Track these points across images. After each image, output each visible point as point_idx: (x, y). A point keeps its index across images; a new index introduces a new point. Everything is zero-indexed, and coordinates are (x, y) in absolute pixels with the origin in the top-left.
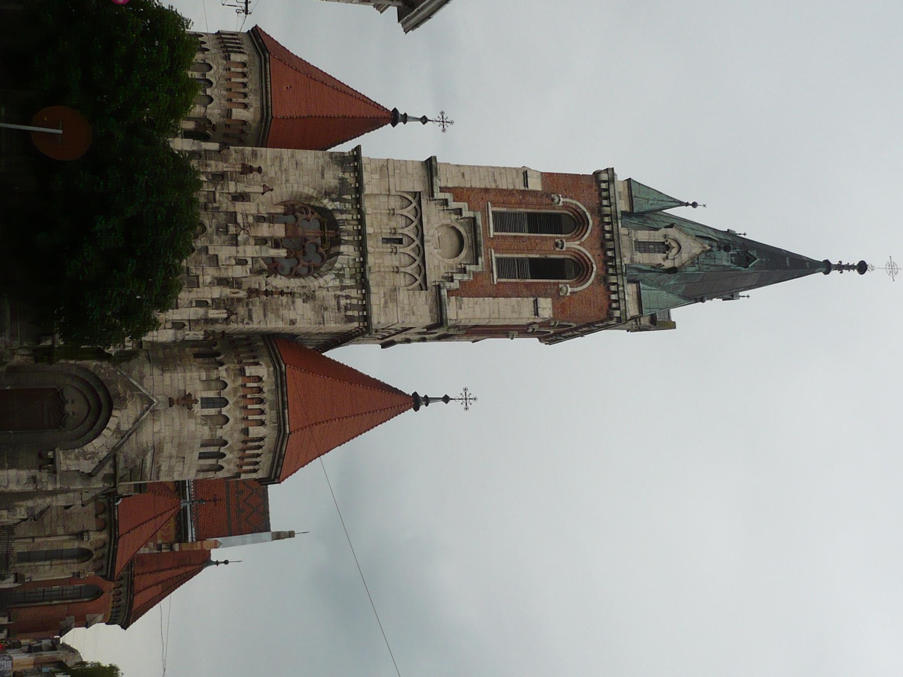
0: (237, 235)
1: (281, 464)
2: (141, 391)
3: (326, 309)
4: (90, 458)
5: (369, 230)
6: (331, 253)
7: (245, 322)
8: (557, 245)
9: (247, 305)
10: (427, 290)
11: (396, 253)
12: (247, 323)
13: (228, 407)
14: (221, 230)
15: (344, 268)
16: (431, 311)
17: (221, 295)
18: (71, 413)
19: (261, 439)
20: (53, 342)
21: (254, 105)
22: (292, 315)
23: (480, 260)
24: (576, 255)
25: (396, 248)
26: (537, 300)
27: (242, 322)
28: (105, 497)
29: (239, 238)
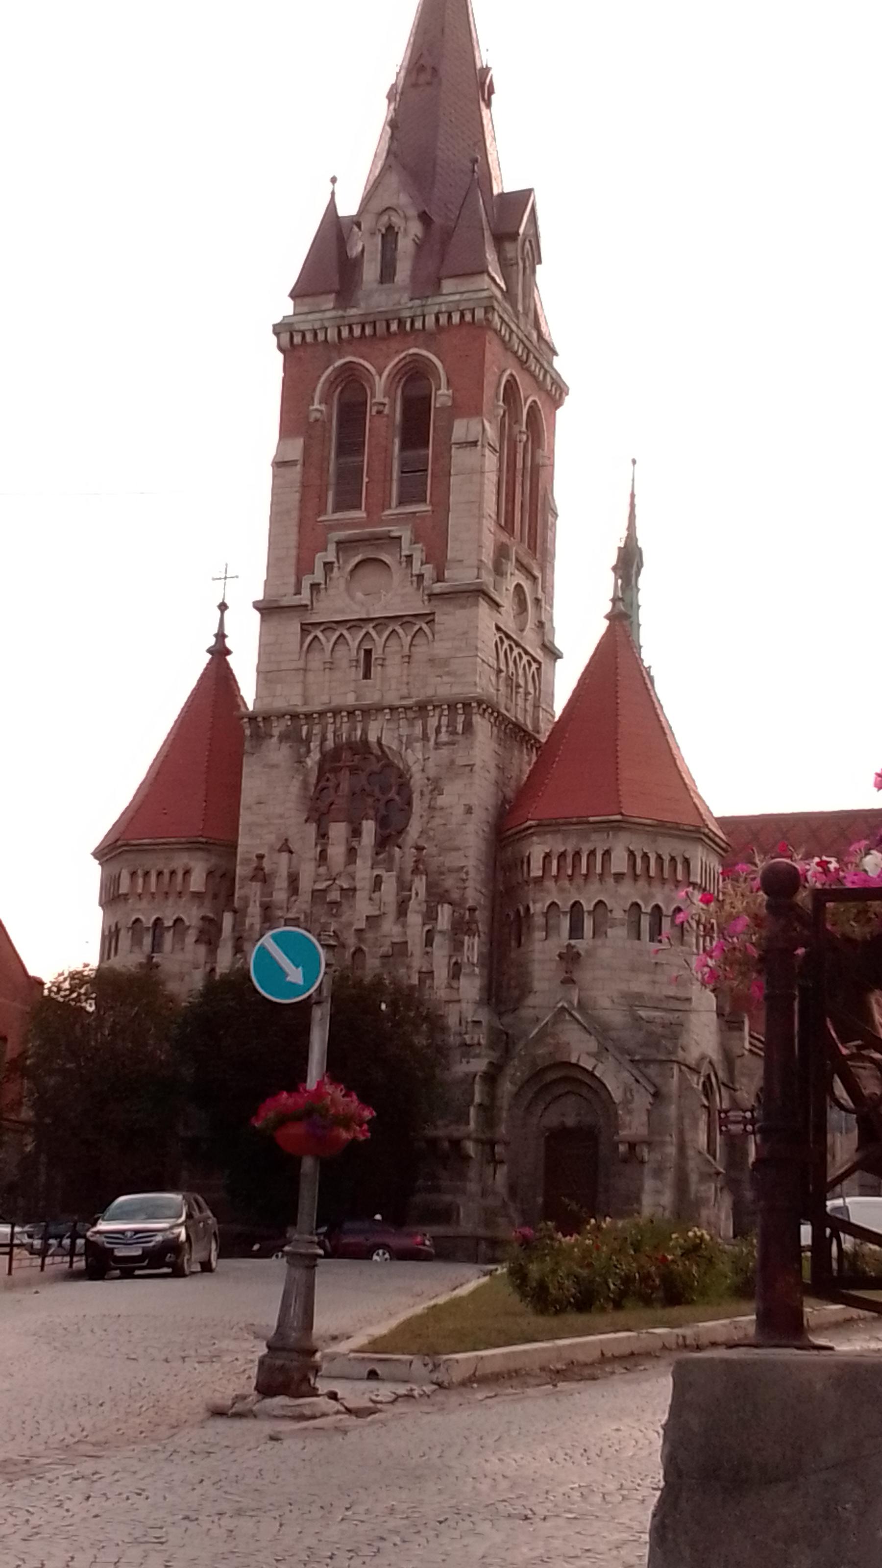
0: (342, 889)
1: (675, 825)
2: (547, 1024)
3: (452, 762)
4: (632, 1096)
5: (350, 700)
6: (380, 753)
7: (464, 877)
8: (379, 412)
9: (442, 873)
10: (434, 613)
11: (384, 659)
12: (467, 873)
14: (335, 911)
15: (400, 735)
16: (463, 607)
17: (417, 912)
18: (579, 1118)
19: (632, 854)
20: (468, 1137)
21: (186, 861)
22: (460, 810)
25: (376, 659)
27: (464, 880)
29: (345, 886)
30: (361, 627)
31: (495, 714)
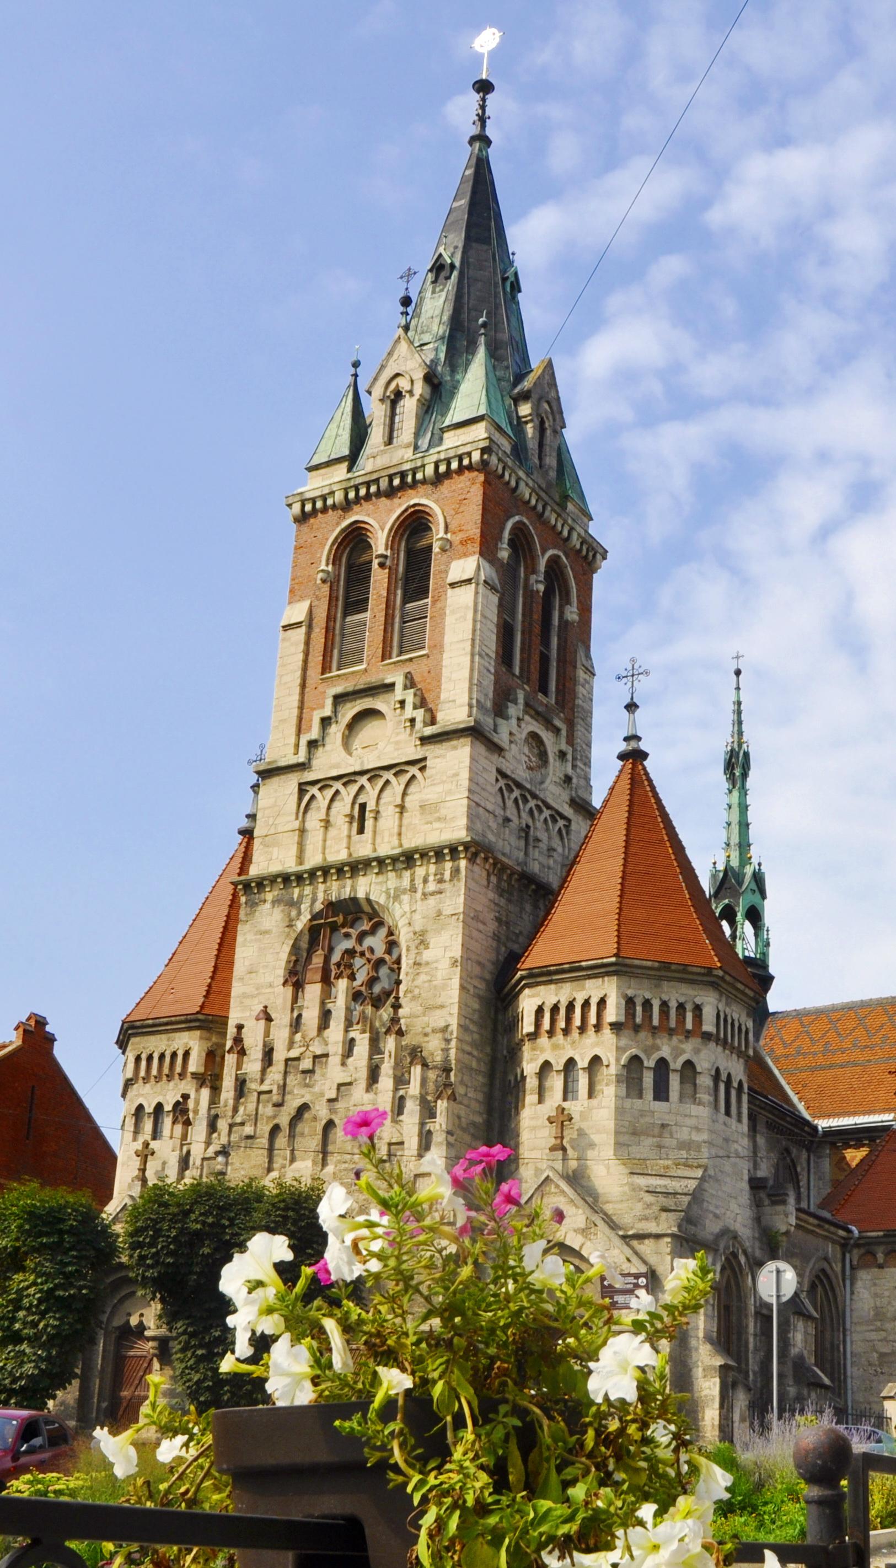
0: (316, 1057)
1: (681, 968)
3: (439, 914)
6: (370, 911)
9: (426, 1035)
10: (425, 759)
12: (452, 1033)
13: (577, 1058)
14: (307, 1081)
15: (388, 889)
16: (455, 748)
19: (630, 1002)
21: (185, 1041)
22: (445, 964)
23: (388, 681)
24: (401, 531)
26: (450, 585)
28: (850, 1252)
29: (318, 1052)
30: (355, 781)
31: (491, 861)
